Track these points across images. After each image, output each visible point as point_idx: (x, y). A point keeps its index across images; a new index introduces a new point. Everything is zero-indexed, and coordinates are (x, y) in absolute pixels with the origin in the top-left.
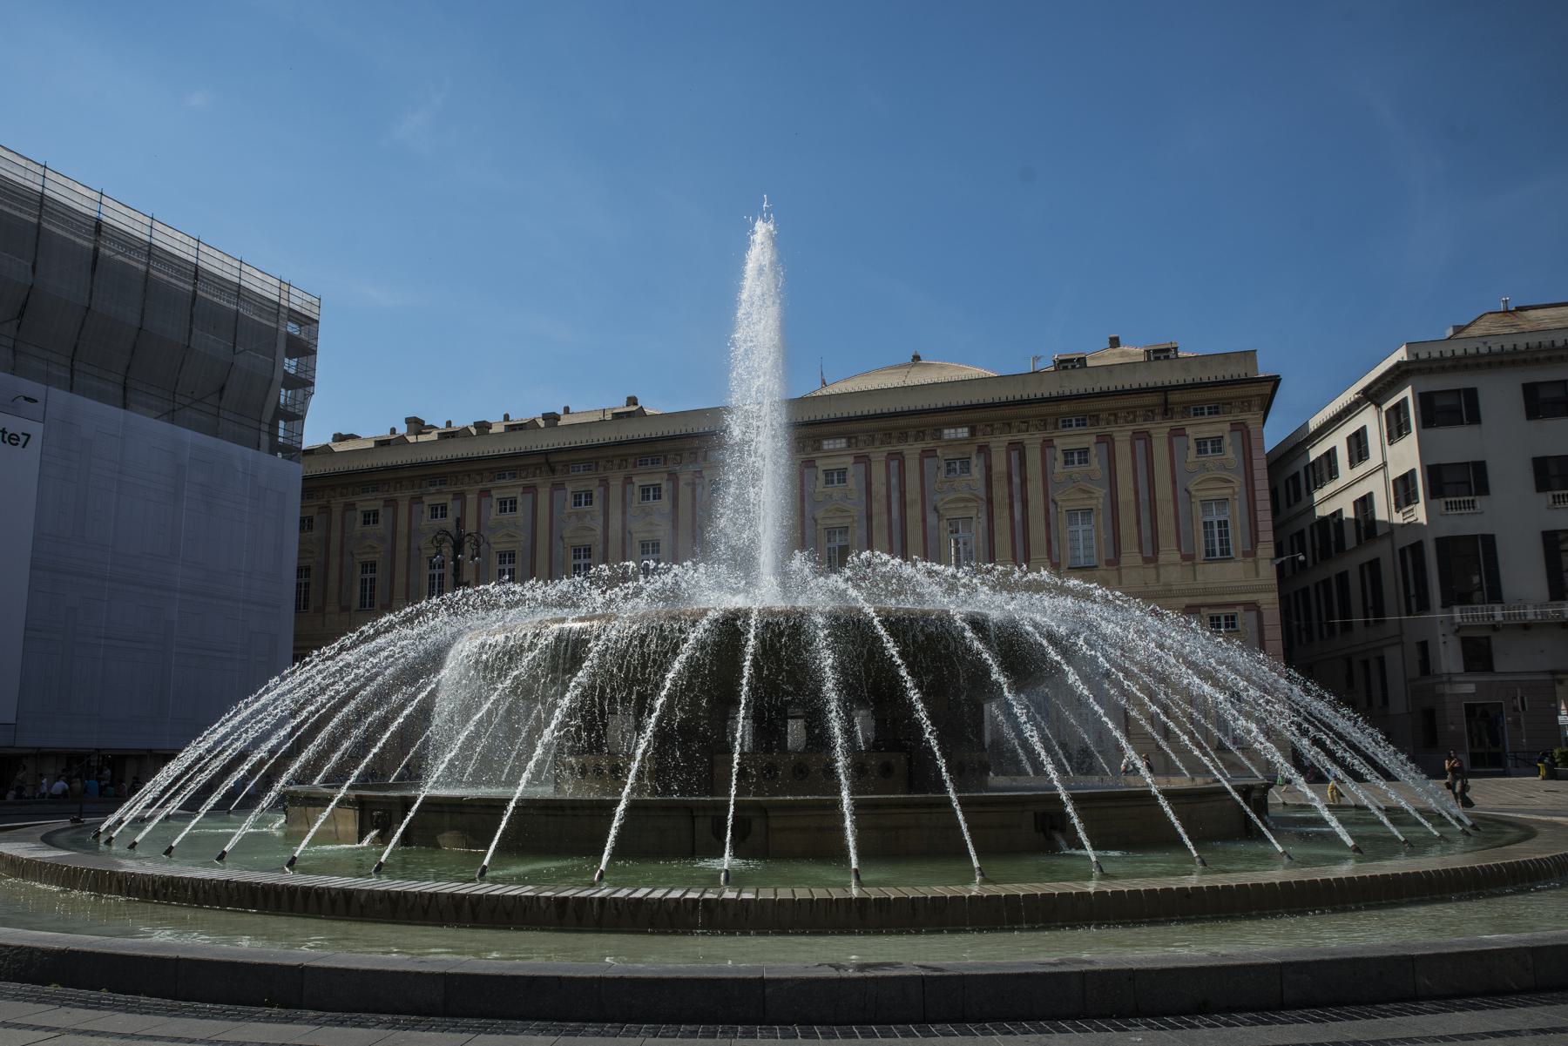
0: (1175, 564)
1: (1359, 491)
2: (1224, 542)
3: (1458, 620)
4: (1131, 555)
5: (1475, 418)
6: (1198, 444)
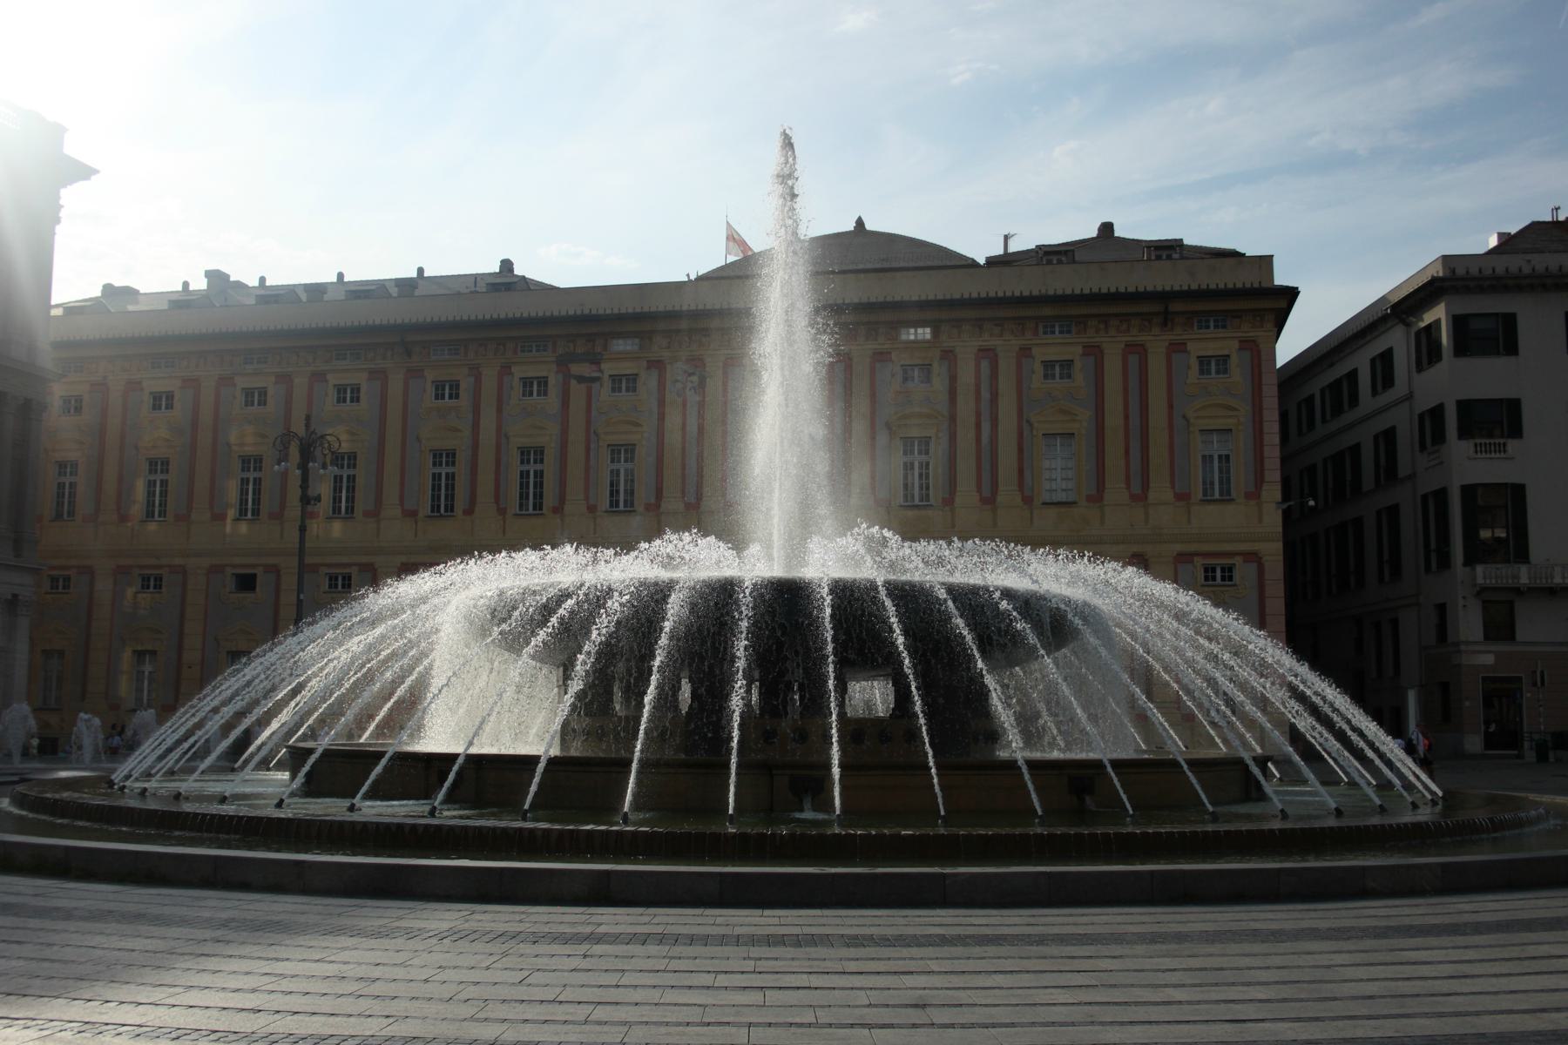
1: (1381, 424)
2: (1225, 482)
3: (1480, 581)
5: (1512, 349)
6: (1201, 363)
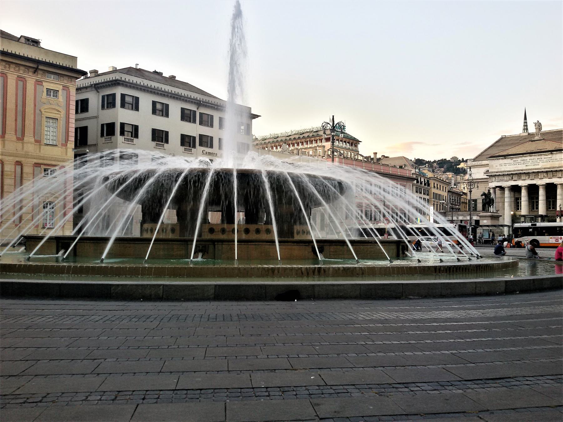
0: (31, 143)
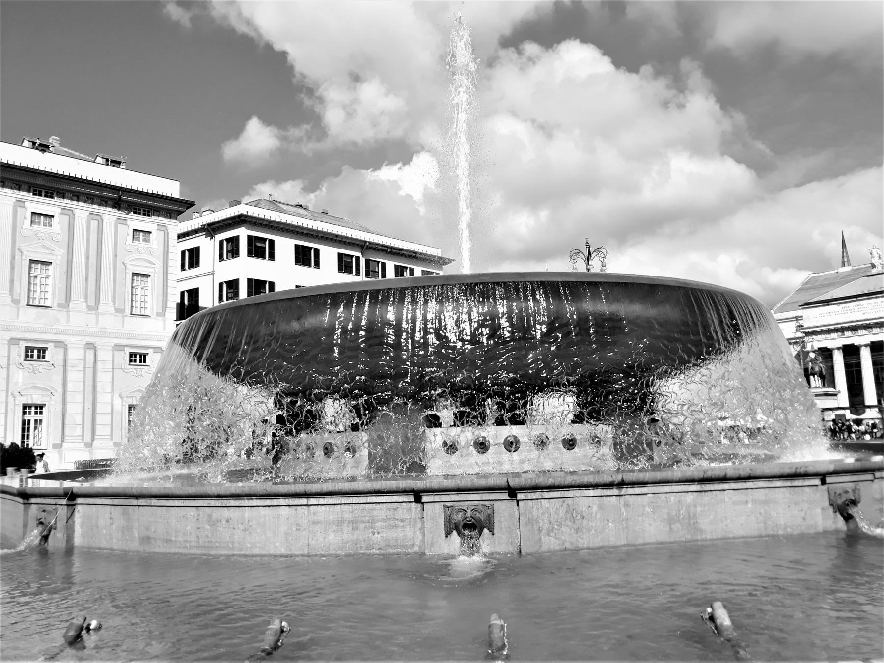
0: (110, 314)
4: (78, 303)
